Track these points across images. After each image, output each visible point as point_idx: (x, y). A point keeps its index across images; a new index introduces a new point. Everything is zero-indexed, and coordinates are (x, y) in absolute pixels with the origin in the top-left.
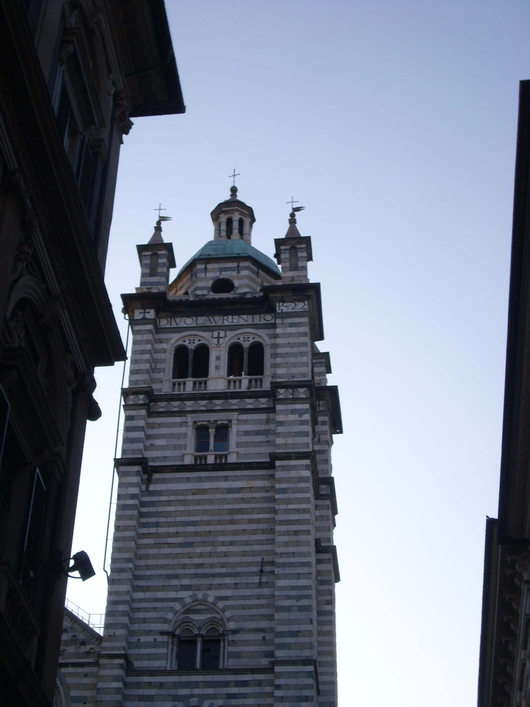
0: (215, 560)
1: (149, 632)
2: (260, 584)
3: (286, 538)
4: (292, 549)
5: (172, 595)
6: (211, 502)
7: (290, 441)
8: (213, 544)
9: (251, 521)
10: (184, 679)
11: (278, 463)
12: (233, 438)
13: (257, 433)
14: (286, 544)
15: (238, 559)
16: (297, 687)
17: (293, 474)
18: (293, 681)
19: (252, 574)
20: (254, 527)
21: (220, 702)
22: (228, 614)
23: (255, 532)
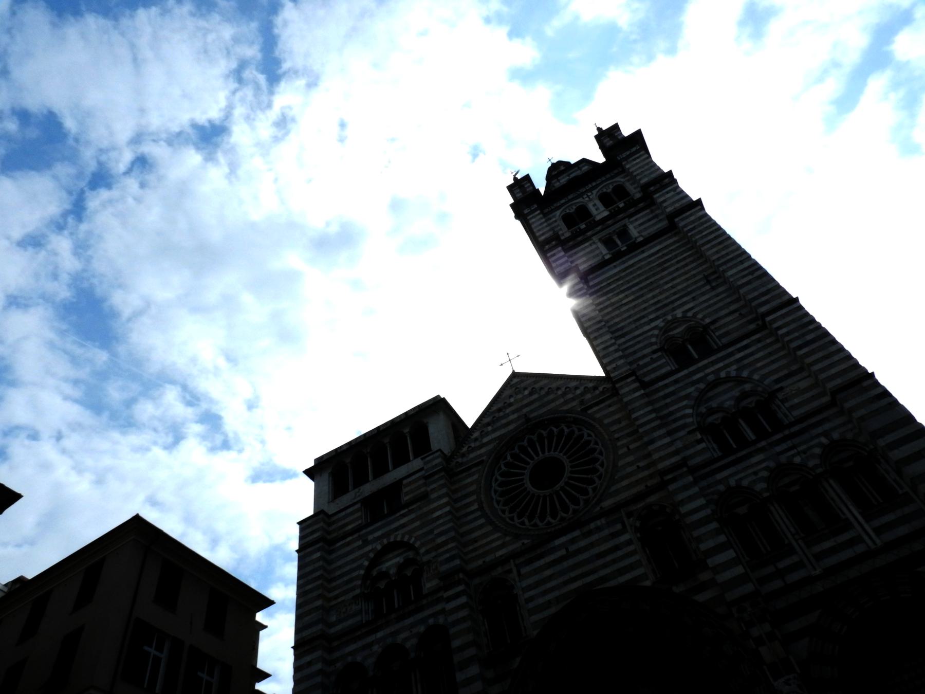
0: (668, 294)
1: (644, 356)
2: (713, 288)
3: (715, 250)
4: (724, 253)
5: (647, 328)
6: (640, 268)
7: (677, 205)
8: (658, 287)
9: (678, 262)
10: (691, 369)
11: (676, 220)
12: (634, 231)
13: (649, 220)
14: (717, 252)
15: (685, 285)
16: (794, 321)
17: (692, 218)
18: (790, 318)
19: (703, 286)
20: (682, 264)
21: (734, 367)
22: (700, 316)
23: (686, 265)
